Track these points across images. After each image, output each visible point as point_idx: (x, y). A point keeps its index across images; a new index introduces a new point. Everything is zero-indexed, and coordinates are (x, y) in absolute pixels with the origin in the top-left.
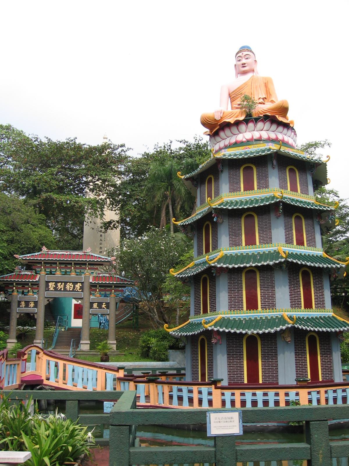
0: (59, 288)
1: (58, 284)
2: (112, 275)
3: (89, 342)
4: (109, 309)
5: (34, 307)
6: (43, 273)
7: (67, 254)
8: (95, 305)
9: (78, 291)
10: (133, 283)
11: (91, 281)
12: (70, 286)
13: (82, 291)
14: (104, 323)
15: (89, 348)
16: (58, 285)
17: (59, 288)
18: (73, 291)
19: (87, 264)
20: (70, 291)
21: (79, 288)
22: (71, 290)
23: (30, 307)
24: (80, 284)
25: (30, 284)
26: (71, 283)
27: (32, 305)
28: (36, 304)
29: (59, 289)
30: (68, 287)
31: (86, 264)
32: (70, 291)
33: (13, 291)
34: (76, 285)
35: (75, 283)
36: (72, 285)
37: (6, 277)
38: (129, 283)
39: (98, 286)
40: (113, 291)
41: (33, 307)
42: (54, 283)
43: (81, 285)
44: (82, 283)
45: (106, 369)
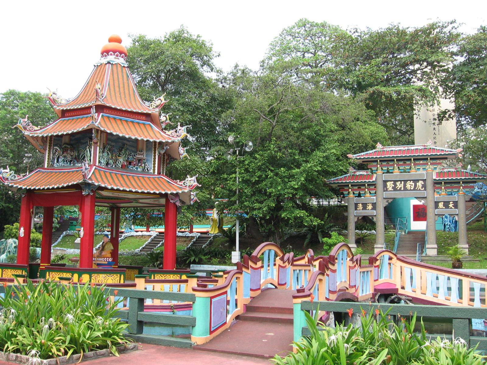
2: (459, 170)
3: (436, 246)
4: (457, 208)
5: (372, 209)
6: (380, 172)
7: (404, 149)
8: (441, 205)
9: (420, 190)
10: (485, 178)
11: (434, 177)
13: (425, 190)
14: (450, 225)
15: (436, 253)
18: (414, 189)
19: (429, 159)
20: (411, 190)
21: (421, 186)
22: (412, 189)
23: (368, 210)
25: (366, 185)
26: (412, 182)
27: (370, 207)
28: (374, 206)
30: (408, 186)
31: (427, 159)
32: (411, 190)
33: (349, 193)
34: (417, 184)
35: (416, 181)
36: (413, 184)
37: (341, 179)
38: (481, 178)
39: (443, 183)
40: (461, 187)
41: (371, 210)
42: (393, 182)
43: (423, 183)
44: (424, 181)
45: (473, 277)
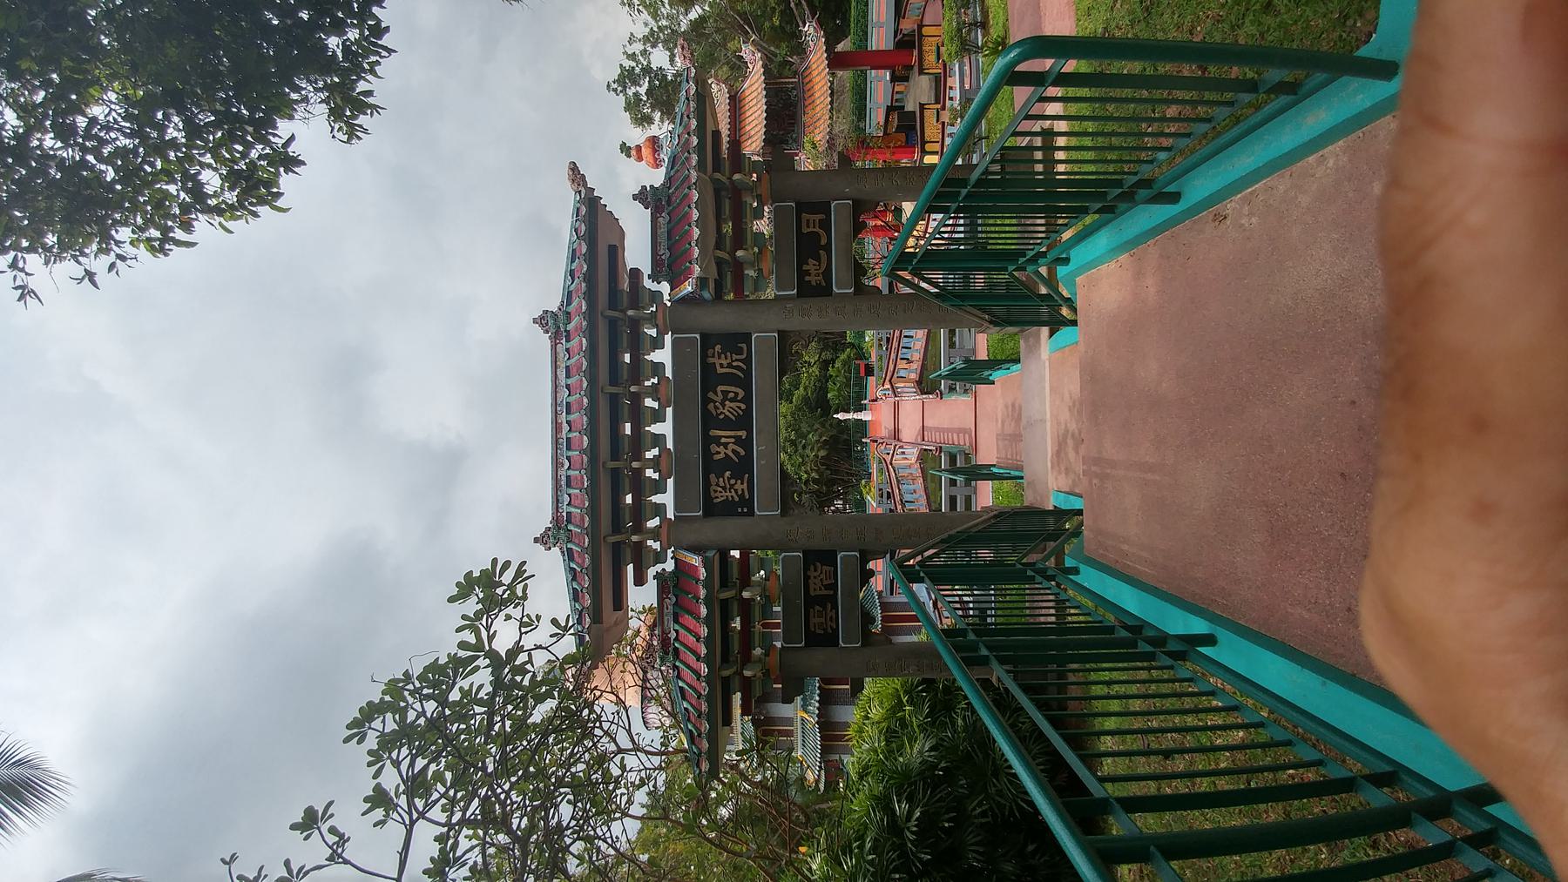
0: (733, 451)
1: (717, 457)
12: (725, 398)
13: (746, 337)
16: (722, 456)
17: (733, 451)
24: (710, 352)
26: (711, 395)
29: (743, 453)
32: (747, 400)
36: (720, 388)
44: (708, 340)
